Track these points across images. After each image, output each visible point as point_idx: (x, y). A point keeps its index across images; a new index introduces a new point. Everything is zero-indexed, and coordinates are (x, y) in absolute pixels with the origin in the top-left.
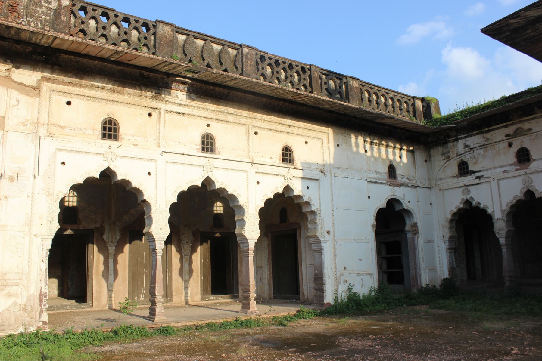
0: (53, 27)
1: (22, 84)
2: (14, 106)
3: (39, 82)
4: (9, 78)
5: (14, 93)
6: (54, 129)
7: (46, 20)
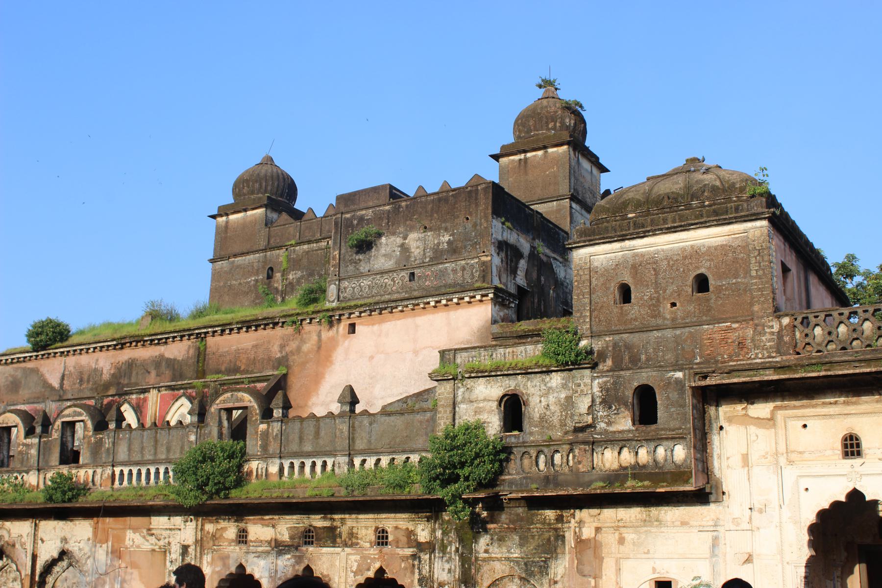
0: (779, 352)
1: (758, 418)
2: (754, 441)
3: (773, 413)
4: (746, 415)
5: (752, 429)
6: (792, 455)
7: (771, 347)
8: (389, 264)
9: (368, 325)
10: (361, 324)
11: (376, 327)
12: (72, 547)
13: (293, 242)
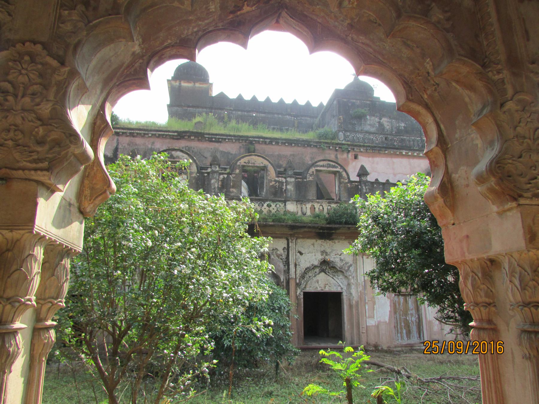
8: (373, 130)
9: (366, 157)
10: (361, 155)
11: (370, 159)
12: (331, 258)
13: (232, 109)
